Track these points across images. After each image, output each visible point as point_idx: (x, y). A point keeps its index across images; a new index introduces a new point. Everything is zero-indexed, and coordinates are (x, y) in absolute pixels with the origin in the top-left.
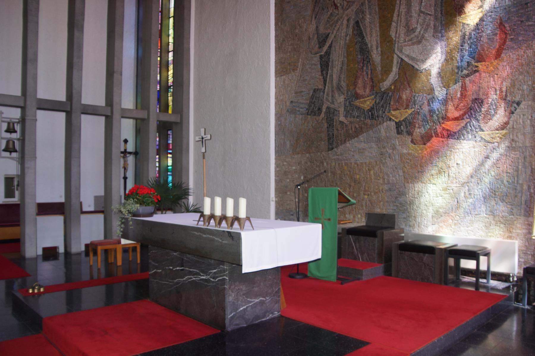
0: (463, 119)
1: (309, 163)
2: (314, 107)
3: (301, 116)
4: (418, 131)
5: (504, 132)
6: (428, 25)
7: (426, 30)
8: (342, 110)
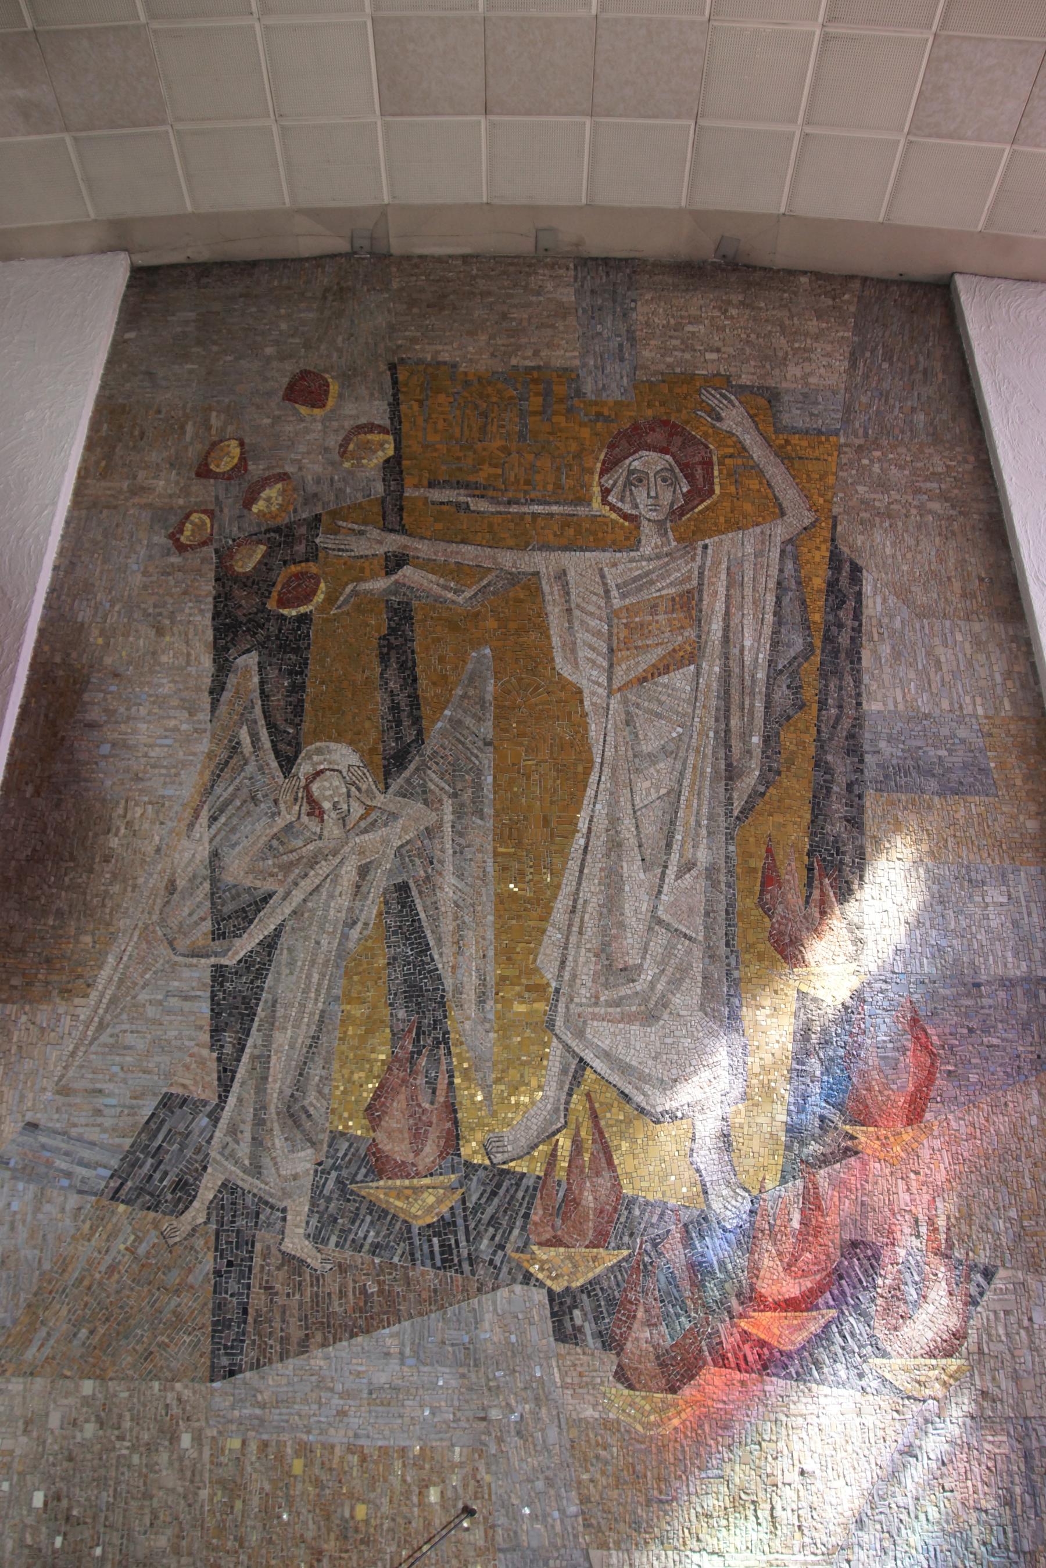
0: (814, 1307)
1: (90, 1429)
3: (73, 1200)
4: (642, 1339)
5: (953, 1364)
6: (683, 970)
7: (676, 983)
8: (299, 1209)
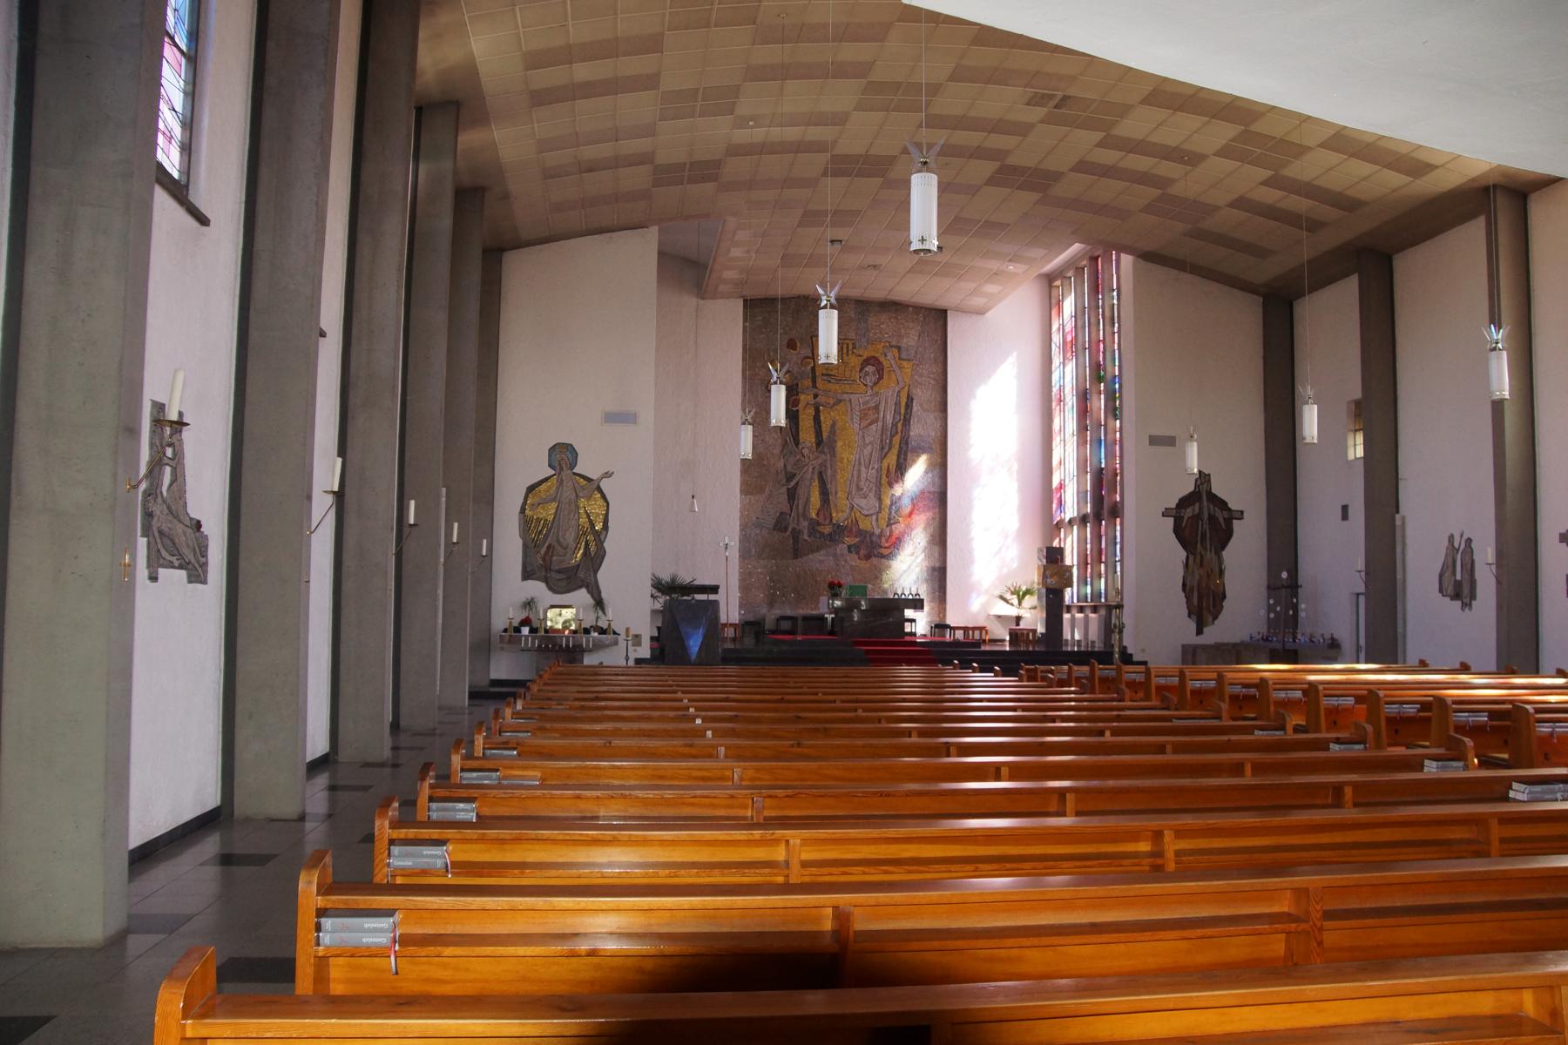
2: (780, 525)
